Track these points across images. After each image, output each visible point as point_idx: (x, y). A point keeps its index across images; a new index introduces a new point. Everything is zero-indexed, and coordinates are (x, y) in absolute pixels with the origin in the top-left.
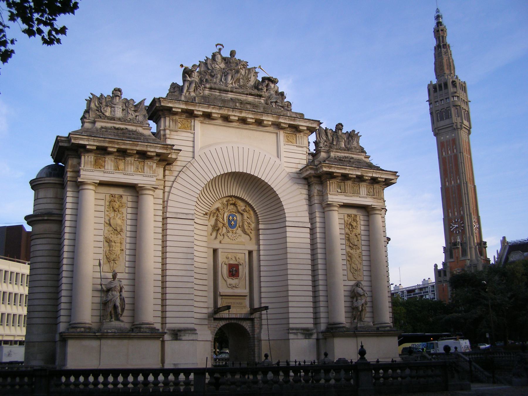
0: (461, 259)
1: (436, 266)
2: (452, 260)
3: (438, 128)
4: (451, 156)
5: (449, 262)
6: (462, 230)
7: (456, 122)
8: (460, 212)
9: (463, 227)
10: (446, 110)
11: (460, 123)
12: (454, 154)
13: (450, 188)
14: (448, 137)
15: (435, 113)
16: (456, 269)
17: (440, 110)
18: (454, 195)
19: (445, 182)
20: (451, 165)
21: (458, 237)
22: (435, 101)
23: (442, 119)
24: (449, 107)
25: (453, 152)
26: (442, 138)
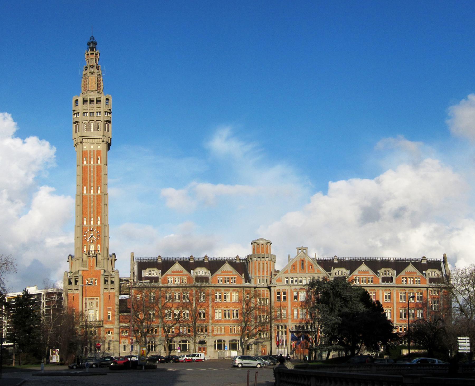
4: (94, 166)
8: (97, 221)
12: (97, 164)
13: (88, 197)
14: (92, 147)
18: (92, 205)
20: (92, 174)
21: (92, 246)
22: (84, 112)
23: (89, 129)
25: (97, 162)
26: (85, 147)
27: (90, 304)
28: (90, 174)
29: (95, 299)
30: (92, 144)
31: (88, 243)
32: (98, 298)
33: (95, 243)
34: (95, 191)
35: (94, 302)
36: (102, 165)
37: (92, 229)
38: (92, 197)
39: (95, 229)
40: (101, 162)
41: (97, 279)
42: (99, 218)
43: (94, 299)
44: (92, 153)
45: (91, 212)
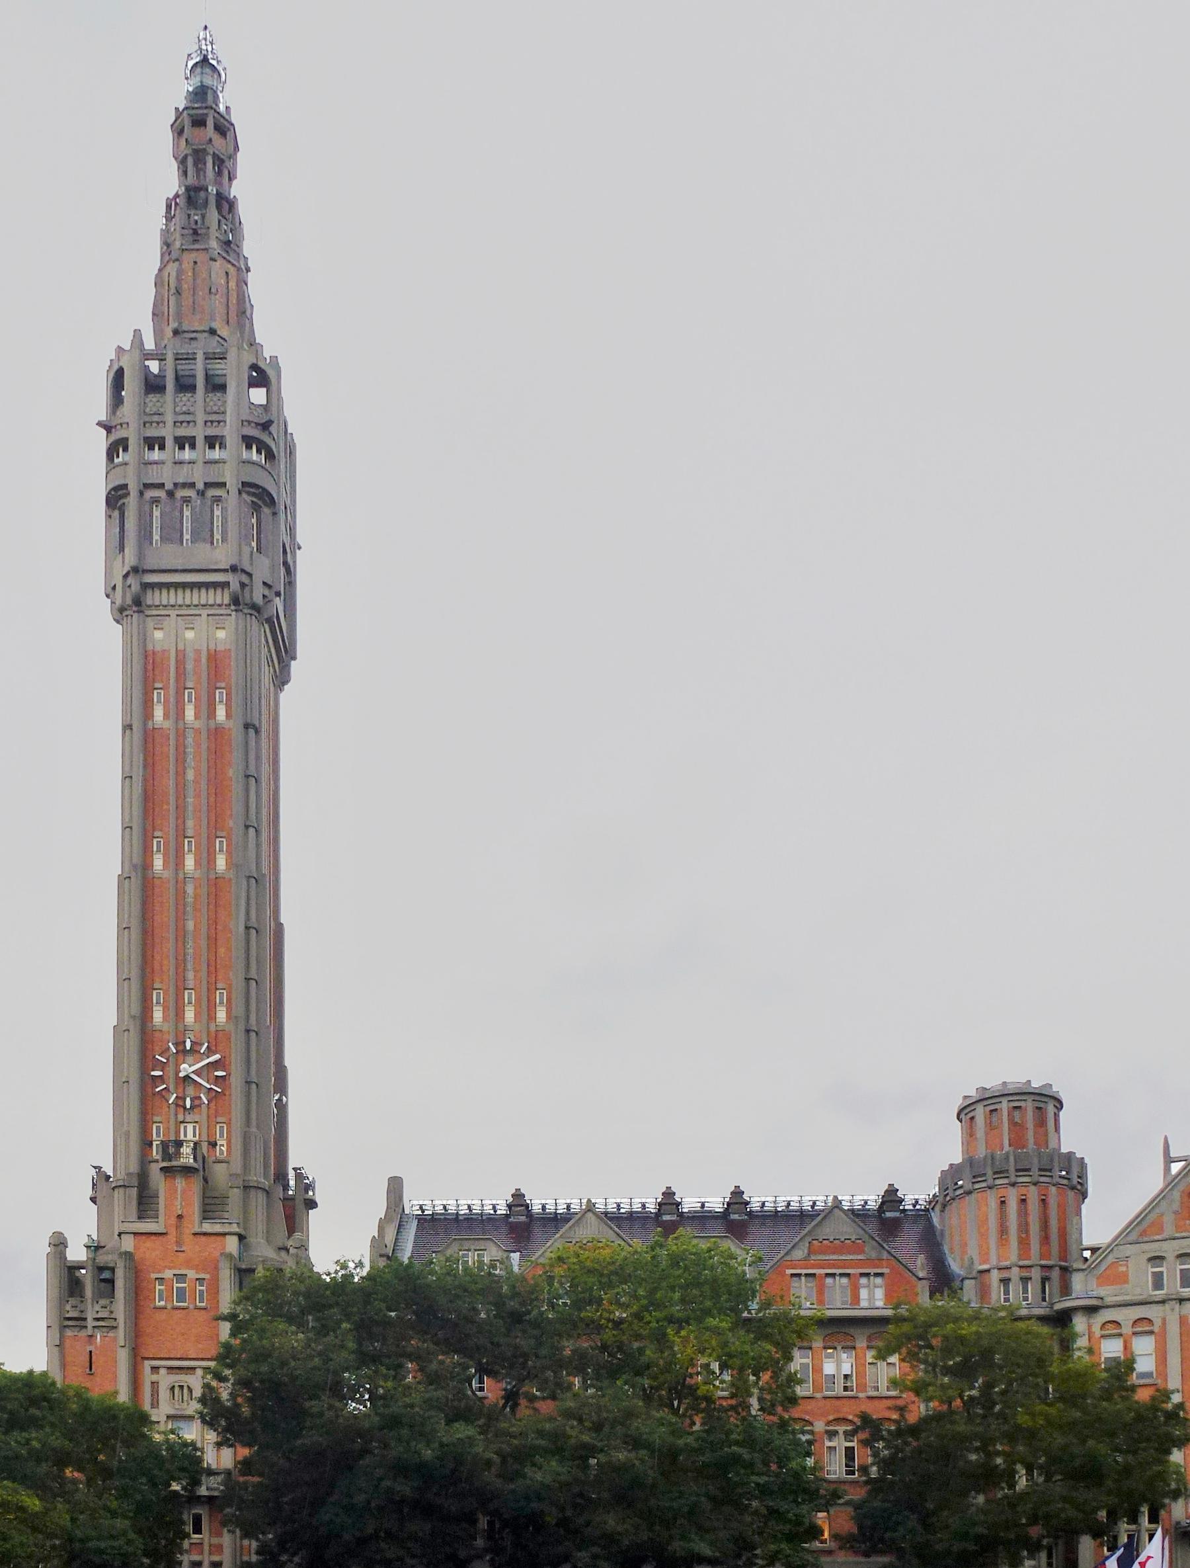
1: (59, 1244)
3: (145, 571)
4: (197, 732)
11: (264, 583)
12: (212, 724)
15: (141, 493)
17: (169, 486)
19: (147, 851)
23: (172, 534)
27: (177, 1390)
28: (180, 773)
29: (199, 1372)
30: (188, 614)
36: (235, 729)
38: (190, 889)
39: (202, 1044)
40: (228, 716)
41: (207, 1276)
42: (220, 996)
43: (194, 1369)
44: (190, 666)
45: (185, 961)
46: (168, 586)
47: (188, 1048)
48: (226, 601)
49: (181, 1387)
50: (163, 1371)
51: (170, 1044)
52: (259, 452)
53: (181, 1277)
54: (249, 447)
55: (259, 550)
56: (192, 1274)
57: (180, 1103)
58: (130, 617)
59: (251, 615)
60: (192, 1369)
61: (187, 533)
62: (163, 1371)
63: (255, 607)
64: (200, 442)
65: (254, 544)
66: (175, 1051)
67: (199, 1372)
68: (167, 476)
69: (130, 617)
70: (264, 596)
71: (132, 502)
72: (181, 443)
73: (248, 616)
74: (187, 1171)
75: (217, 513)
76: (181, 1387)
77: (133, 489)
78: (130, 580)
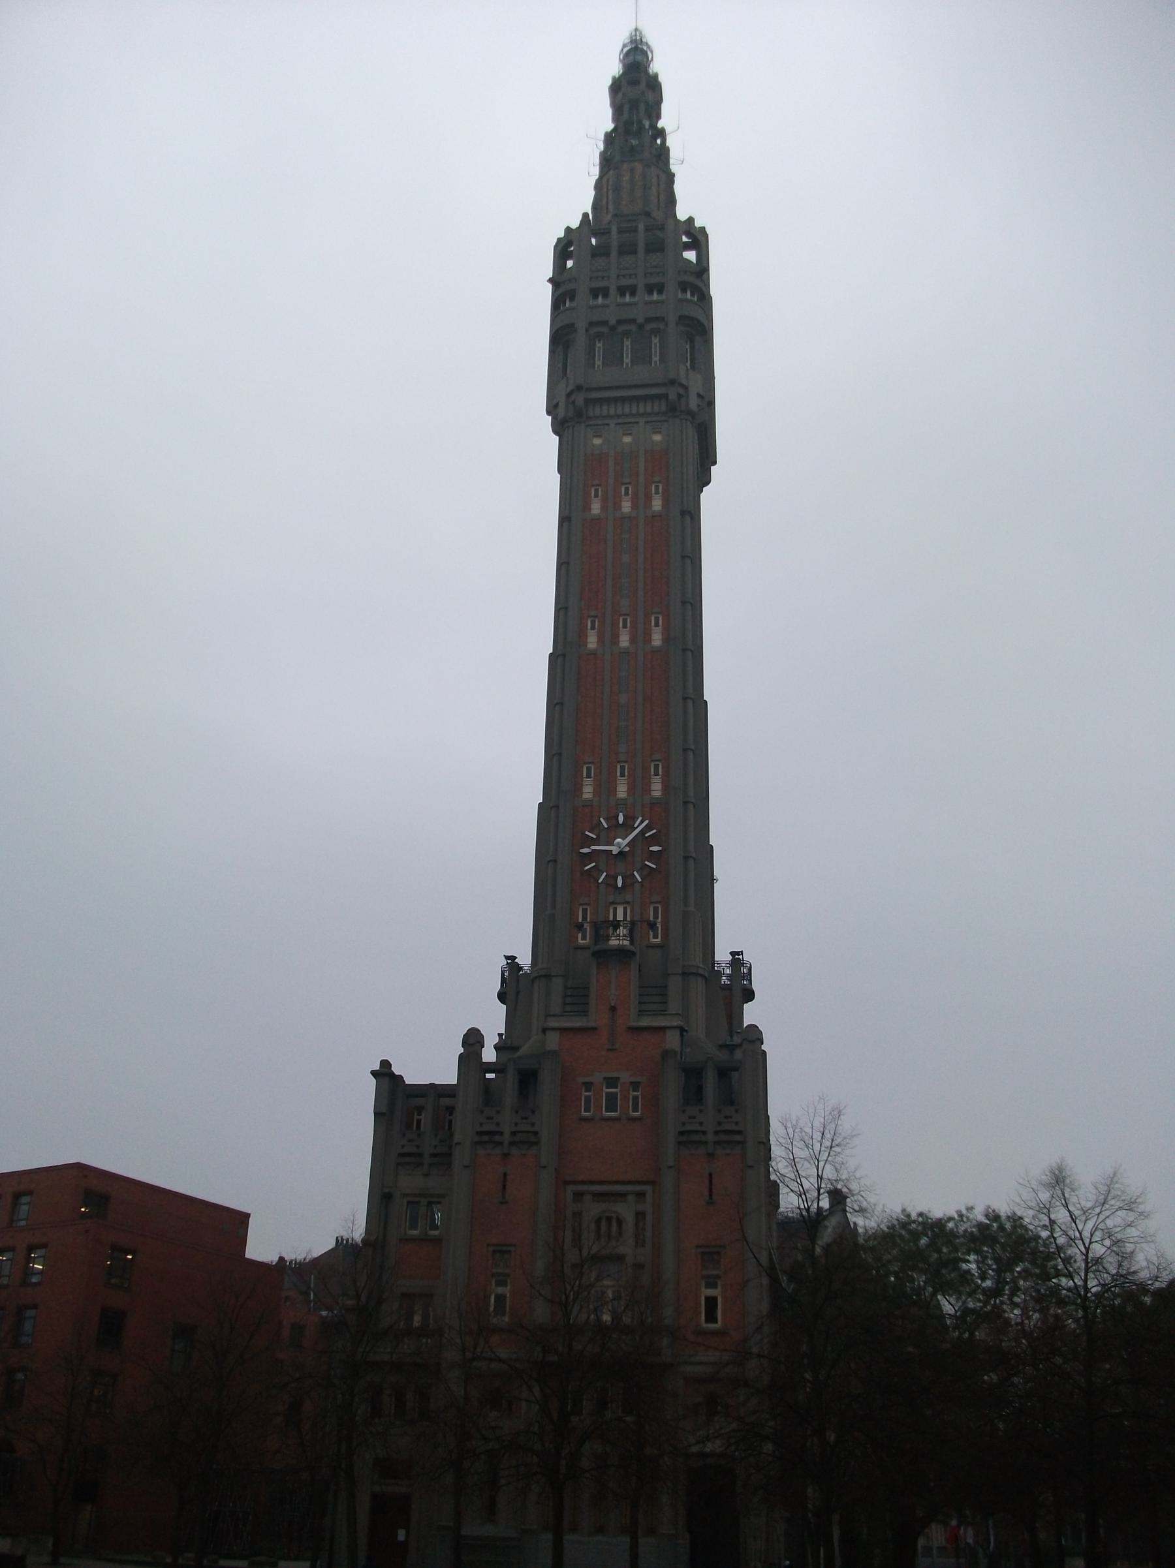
0: (633, 1024)
2: (577, 1023)
3: (589, 390)
5: (562, 1030)
6: (648, 873)
7: (684, 382)
9: (652, 856)
10: (641, 327)
11: (699, 395)
14: (627, 440)
15: (587, 330)
16: (597, 1078)
24: (661, 319)
27: (603, 1223)
29: (631, 1198)
31: (602, 887)
32: (648, 1189)
33: (637, 886)
34: (641, 636)
35: (626, 1211)
37: (621, 819)
46: (608, 401)
47: (621, 821)
48: (664, 408)
49: (609, 1219)
50: (588, 1198)
51: (602, 820)
52: (692, 295)
53: (612, 1082)
54: (684, 291)
55: (693, 367)
56: (625, 1077)
57: (611, 882)
58: (571, 428)
59: (686, 420)
60: (623, 1195)
61: (627, 357)
62: (588, 1198)
63: (690, 413)
64: (641, 288)
65: (688, 364)
66: (606, 826)
67: (631, 1198)
68: (612, 317)
69: (571, 428)
70: (699, 406)
71: (581, 338)
72: (622, 291)
73: (684, 421)
74: (623, 954)
75: (656, 340)
76: (609, 1219)
77: (581, 326)
78: (572, 398)
